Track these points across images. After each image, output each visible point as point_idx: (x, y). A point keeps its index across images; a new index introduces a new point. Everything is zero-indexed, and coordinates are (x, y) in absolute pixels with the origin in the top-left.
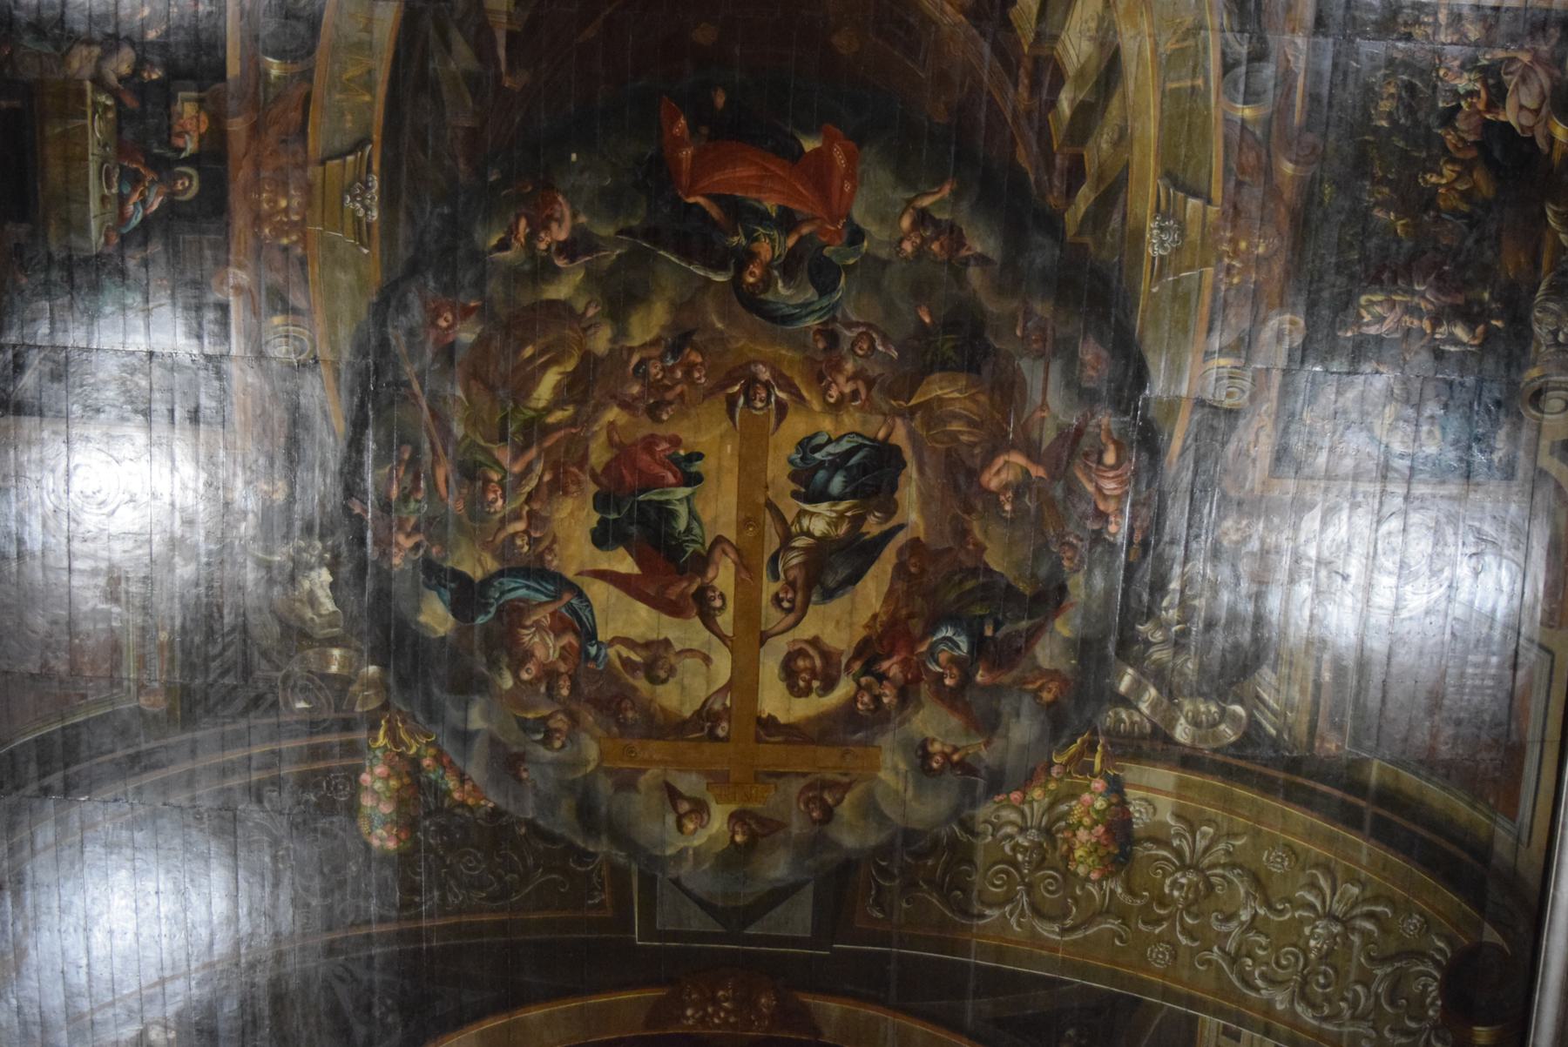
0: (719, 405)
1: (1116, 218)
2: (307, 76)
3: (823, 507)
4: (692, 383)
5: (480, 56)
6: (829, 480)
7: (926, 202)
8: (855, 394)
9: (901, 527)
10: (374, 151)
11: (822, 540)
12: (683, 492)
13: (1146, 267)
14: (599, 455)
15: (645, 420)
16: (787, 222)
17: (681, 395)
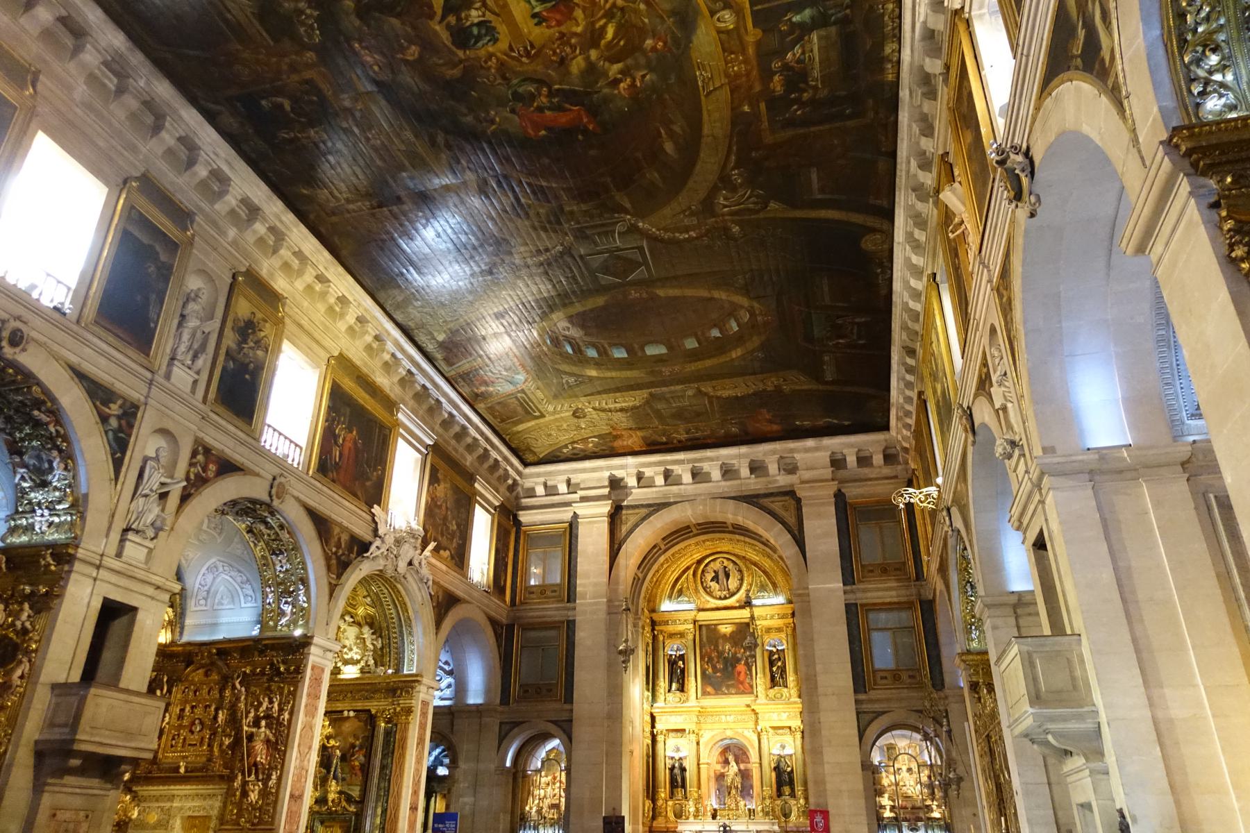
0: (537, 44)
1: (427, 139)
2: (732, 109)
3: (476, 21)
4: (551, 49)
5: (671, 130)
6: (479, 32)
7: (494, 127)
8: (486, 62)
9: (440, 22)
10: (703, 94)
11: (469, 8)
12: (537, 10)
13: (406, 127)
14: (578, 13)
15: (565, 31)
16: (540, 109)
17: (554, 43)
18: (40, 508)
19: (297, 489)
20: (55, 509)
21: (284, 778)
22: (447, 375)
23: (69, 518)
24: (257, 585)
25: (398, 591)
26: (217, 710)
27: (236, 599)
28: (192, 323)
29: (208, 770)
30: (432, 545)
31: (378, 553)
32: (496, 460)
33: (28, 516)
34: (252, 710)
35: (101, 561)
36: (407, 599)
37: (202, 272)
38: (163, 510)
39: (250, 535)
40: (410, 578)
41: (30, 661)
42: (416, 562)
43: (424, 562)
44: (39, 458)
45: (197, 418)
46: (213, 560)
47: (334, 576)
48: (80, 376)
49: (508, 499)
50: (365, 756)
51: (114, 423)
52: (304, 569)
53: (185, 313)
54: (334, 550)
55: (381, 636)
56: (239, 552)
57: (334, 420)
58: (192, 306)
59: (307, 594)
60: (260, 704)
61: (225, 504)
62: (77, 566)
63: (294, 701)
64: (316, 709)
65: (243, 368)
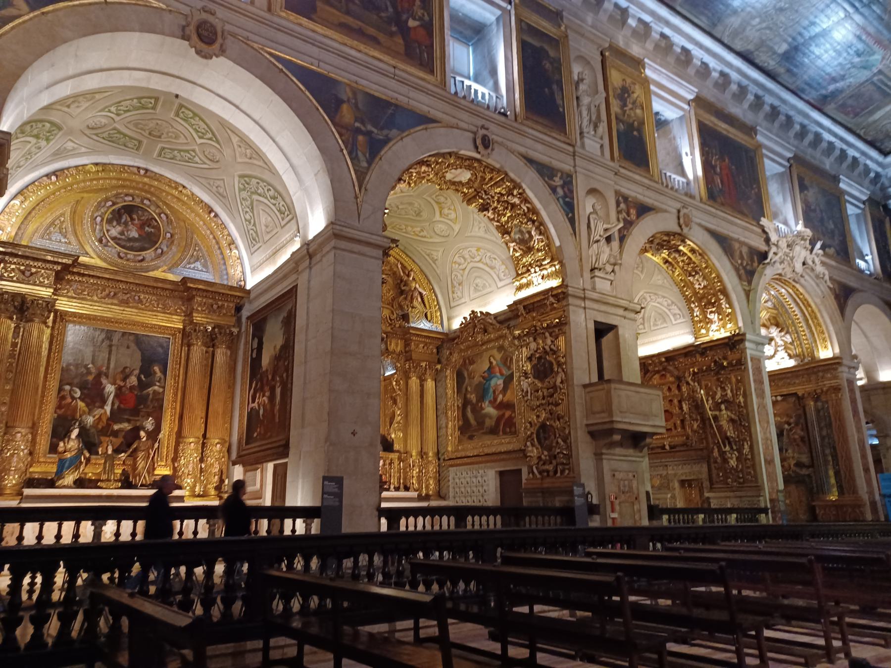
18: (532, 267)
19: (698, 217)
20: (542, 265)
21: (755, 447)
22: (792, 87)
23: (553, 269)
24: (682, 303)
25: (797, 290)
26: (680, 402)
27: (667, 319)
28: (586, 100)
29: (687, 446)
30: (819, 245)
31: (777, 258)
32: (854, 159)
33: (526, 275)
34: (710, 398)
35: (584, 294)
36: (807, 296)
37: (581, 58)
38: (611, 250)
39: (667, 264)
40: (807, 277)
41: (563, 371)
42: (810, 262)
43: (817, 260)
44: (521, 232)
45: (611, 175)
46: (641, 293)
47: (745, 283)
48: (530, 161)
49: (873, 192)
50: (802, 430)
51: (560, 192)
52: (721, 281)
53: (579, 94)
54: (739, 262)
55: (787, 332)
56: (660, 282)
57: (708, 153)
58: (582, 87)
59: (729, 302)
60: (715, 393)
61: (645, 243)
62: (571, 300)
63: (744, 387)
64: (763, 392)
65: (630, 127)
